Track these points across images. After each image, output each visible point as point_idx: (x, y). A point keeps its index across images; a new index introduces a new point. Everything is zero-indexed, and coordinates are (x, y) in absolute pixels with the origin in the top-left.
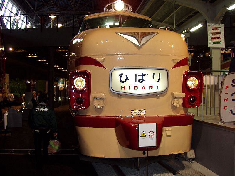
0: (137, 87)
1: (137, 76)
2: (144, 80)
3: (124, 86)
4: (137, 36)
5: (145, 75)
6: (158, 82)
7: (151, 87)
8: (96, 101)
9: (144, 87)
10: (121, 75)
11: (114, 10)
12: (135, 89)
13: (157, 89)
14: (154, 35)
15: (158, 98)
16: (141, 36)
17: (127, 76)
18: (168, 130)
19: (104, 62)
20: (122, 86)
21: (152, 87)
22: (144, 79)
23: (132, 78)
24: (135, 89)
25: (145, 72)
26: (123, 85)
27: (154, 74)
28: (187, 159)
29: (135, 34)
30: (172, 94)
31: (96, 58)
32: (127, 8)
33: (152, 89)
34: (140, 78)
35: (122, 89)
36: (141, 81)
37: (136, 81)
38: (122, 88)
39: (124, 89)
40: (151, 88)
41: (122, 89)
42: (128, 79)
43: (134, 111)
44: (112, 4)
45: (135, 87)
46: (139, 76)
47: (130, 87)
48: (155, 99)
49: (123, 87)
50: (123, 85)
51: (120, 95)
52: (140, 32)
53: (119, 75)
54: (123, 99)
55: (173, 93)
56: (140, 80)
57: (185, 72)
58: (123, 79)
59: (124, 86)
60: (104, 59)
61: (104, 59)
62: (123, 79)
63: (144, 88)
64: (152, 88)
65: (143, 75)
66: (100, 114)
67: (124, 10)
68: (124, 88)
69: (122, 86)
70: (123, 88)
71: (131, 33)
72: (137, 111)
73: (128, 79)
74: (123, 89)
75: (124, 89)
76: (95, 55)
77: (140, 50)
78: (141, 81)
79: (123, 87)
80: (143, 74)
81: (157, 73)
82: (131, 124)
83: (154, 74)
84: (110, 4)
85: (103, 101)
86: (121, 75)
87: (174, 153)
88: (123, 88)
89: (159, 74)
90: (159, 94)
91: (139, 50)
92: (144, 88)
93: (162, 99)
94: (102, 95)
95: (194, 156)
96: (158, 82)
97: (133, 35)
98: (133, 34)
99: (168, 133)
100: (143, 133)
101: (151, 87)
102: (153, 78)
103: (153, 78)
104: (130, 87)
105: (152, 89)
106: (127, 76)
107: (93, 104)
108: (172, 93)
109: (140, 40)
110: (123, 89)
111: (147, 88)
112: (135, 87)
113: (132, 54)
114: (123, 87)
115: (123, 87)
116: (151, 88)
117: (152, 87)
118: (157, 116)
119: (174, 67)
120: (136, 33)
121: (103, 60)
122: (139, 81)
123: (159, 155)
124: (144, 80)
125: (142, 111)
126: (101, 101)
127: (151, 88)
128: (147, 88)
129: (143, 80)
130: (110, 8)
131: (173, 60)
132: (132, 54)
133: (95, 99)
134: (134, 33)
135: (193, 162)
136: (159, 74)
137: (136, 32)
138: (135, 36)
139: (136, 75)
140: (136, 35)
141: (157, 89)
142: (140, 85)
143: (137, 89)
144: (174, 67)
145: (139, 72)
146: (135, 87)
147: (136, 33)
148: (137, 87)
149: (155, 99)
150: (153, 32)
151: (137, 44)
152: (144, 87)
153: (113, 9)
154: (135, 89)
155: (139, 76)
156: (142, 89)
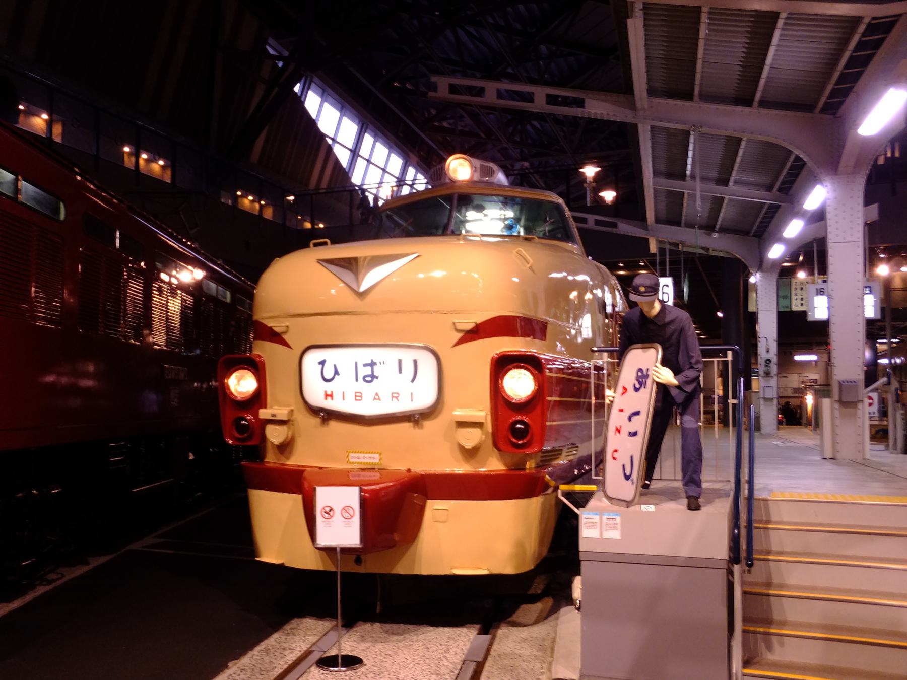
1: (360, 367)
2: (377, 378)
5: (378, 363)
9: (377, 394)
10: (322, 363)
12: (357, 398)
22: (375, 374)
23: (347, 372)
24: (356, 400)
26: (329, 387)
34: (368, 370)
37: (357, 380)
38: (327, 395)
46: (365, 365)
50: (329, 387)
51: (328, 416)
61: (287, 327)
62: (329, 374)
64: (397, 398)
65: (372, 364)
66: (288, 458)
68: (331, 396)
76: (270, 318)
78: (369, 379)
81: (407, 356)
86: (322, 363)
89: (415, 362)
91: (362, 300)
92: (377, 397)
93: (429, 425)
94: (282, 413)
111: (385, 395)
118: (409, 471)
119: (460, 342)
124: (377, 378)
127: (395, 396)
128: (385, 395)
129: (373, 377)
136: (415, 362)
142: (368, 390)
143: (360, 398)
144: (460, 342)
145: (364, 355)
146: (358, 394)
152: (377, 394)
154: (357, 398)
155: (365, 365)
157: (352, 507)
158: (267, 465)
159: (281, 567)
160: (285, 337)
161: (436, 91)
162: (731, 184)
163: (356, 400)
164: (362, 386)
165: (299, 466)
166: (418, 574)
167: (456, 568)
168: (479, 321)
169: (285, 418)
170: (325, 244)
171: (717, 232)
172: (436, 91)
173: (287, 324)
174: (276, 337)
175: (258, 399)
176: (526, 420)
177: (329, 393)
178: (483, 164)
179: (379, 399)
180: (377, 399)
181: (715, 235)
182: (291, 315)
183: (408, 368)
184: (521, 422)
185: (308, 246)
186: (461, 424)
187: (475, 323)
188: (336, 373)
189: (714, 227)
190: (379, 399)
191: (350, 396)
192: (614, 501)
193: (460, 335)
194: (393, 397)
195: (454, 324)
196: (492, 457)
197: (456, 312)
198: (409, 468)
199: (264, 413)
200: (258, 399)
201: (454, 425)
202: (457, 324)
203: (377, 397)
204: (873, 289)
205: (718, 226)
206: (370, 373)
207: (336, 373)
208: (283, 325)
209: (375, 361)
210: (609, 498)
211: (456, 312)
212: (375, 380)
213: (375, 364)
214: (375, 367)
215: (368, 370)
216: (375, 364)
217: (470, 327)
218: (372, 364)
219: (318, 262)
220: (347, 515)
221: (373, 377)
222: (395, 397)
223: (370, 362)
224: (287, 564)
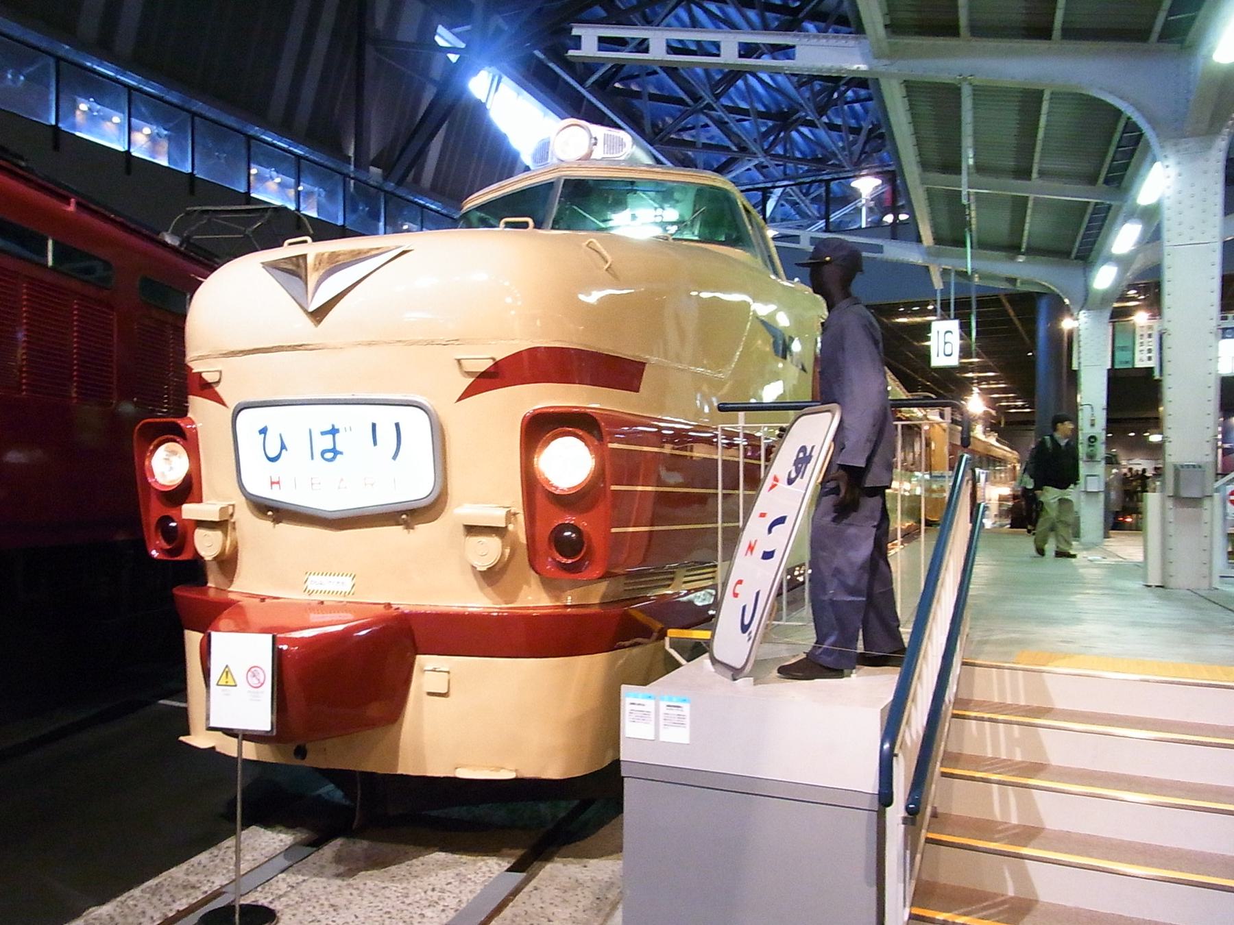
1: (316, 435)
2: (341, 453)
4: (304, 271)
10: (263, 431)
15: (408, 526)
18: (434, 670)
22: (338, 448)
23: (299, 445)
29: (298, 266)
34: (327, 442)
46: (323, 433)
48: (399, 529)
54: (285, 528)
56: (329, 451)
65: (334, 431)
78: (329, 455)
81: (385, 417)
86: (263, 431)
87: (464, 774)
91: (316, 326)
93: (422, 529)
100: (227, 671)
113: (294, 348)
119: (468, 393)
123: (399, 772)
126: (217, 535)
132: (294, 348)
134: (297, 257)
144: (468, 393)
149: (395, 532)
150: (378, 249)
155: (323, 433)
157: (261, 666)
160: (218, 389)
161: (578, 47)
162: (1035, 175)
169: (216, 519)
171: (1023, 254)
172: (578, 47)
174: (207, 389)
175: (188, 489)
176: (583, 524)
177: (275, 480)
178: (610, 133)
181: (1021, 259)
183: (387, 436)
184: (574, 528)
186: (472, 530)
188: (283, 447)
189: (1020, 248)
192: (718, 666)
193: (471, 380)
195: (459, 361)
196: (528, 584)
199: (190, 511)
200: (188, 489)
201: (462, 529)
205: (1024, 246)
207: (283, 447)
209: (336, 427)
210: (714, 661)
212: (339, 456)
213: (337, 431)
214: (337, 435)
215: (327, 442)
216: (337, 431)
218: (334, 431)
219: (263, 267)
220: (254, 682)
221: (335, 452)
224: (218, 749)
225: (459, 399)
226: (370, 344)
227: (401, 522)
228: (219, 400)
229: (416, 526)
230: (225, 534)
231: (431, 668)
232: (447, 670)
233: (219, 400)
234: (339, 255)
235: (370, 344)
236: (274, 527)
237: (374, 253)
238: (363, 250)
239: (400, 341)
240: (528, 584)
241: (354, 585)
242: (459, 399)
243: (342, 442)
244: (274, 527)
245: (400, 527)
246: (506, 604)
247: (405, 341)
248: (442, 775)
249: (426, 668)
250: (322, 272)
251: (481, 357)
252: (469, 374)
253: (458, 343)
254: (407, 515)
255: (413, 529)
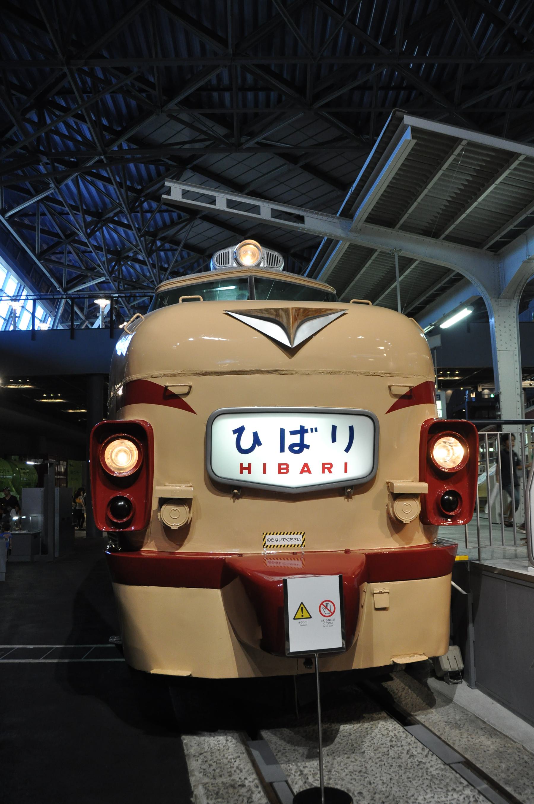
0: (285, 466)
1: (287, 434)
2: (308, 447)
3: (250, 465)
5: (309, 431)
6: (347, 450)
7: (326, 466)
8: (166, 508)
9: (306, 465)
10: (239, 431)
11: (235, 265)
12: (282, 471)
13: (346, 471)
14: (333, 317)
15: (349, 496)
16: (295, 319)
17: (255, 435)
19: (189, 396)
20: (241, 465)
21: (329, 466)
22: (306, 443)
24: (280, 472)
25: (308, 421)
26: (246, 459)
27: (334, 428)
28: (439, 675)
29: (278, 315)
30: (389, 486)
31: (167, 384)
32: (272, 261)
33: (330, 472)
34: (296, 439)
35: (241, 472)
36: (297, 448)
37: (282, 450)
38: (242, 468)
39: (250, 472)
40: (326, 471)
41: (241, 472)
42: (260, 444)
43: (271, 537)
44: (231, 250)
45: (282, 467)
46: (293, 433)
47: (265, 465)
48: (340, 500)
49: (246, 465)
50: (246, 459)
52: (292, 308)
53: (235, 432)
54: (245, 503)
55: (392, 484)
57: (426, 422)
58: (246, 443)
59: (250, 465)
60: (190, 387)
61: (190, 387)
62: (246, 443)
63: (306, 469)
65: (302, 431)
66: (180, 545)
67: (262, 265)
68: (249, 469)
69: (241, 465)
70: (246, 469)
71: (266, 310)
72: (278, 537)
73: (260, 444)
74: (245, 472)
75: (250, 472)
76: (165, 376)
77: (293, 359)
78: (297, 448)
79: (246, 465)
80: (302, 427)
82: (266, 577)
83: (334, 428)
84: (226, 250)
85: (187, 508)
86: (239, 431)
88: (246, 469)
89: (351, 429)
90: (351, 487)
91: (290, 359)
92: (306, 469)
95: (462, 666)
96: (347, 450)
97: (271, 317)
98: (272, 314)
99: (381, 601)
101: (326, 466)
102: (334, 440)
103: (334, 440)
104: (265, 465)
105: (330, 472)
106: (255, 435)
107: (159, 517)
108: (388, 483)
109: (292, 331)
110: (245, 472)
111: (316, 468)
112: (280, 465)
114: (244, 466)
115: (244, 466)
116: (326, 471)
117: (331, 465)
118: (347, 551)
119: (393, 408)
120: (281, 312)
121: (186, 390)
122: (291, 448)
124: (308, 447)
125: (295, 536)
127: (327, 467)
128: (316, 468)
129: (302, 446)
130: (224, 260)
131: (389, 387)
133: (163, 501)
134: (277, 310)
135: (457, 683)
137: (282, 309)
138: (278, 319)
139: (282, 431)
140: (282, 317)
141: (346, 471)
143: (285, 471)
144: (393, 408)
146: (282, 467)
147: (280, 310)
148: (285, 466)
150: (331, 310)
151: (285, 340)
152: (306, 465)
153: (232, 264)
154: (282, 471)
155: (293, 433)
156: (302, 471)
158: (142, 554)
159: (189, 679)
160: (187, 400)
163: (280, 472)
164: (288, 457)
165: (198, 554)
166: (357, 668)
167: (395, 656)
168: (415, 384)
170: (198, 300)
173: (190, 383)
179: (309, 471)
180: (306, 471)
182: (196, 374)
185: (177, 302)
186: (397, 497)
187: (410, 387)
188: (257, 441)
190: (309, 471)
191: (273, 469)
193: (396, 400)
194: (324, 469)
197: (389, 375)
198: (347, 548)
202: (392, 388)
203: (306, 469)
204: (441, 398)
206: (298, 441)
207: (257, 441)
208: (187, 384)
211: (389, 375)
212: (305, 449)
213: (306, 431)
214: (306, 435)
216: (306, 431)
217: (404, 391)
222: (327, 468)
223: (299, 429)
224: (194, 676)
225: (389, 411)
226: (331, 373)
227: (346, 494)
228: (187, 408)
229: (353, 497)
230: (190, 509)
231: (379, 592)
232: (388, 591)
233: (187, 408)
234: (309, 311)
235: (331, 373)
236: (234, 502)
237: (329, 312)
238: (323, 309)
239: (352, 372)
240: (419, 533)
241: (304, 540)
242: (389, 411)
243: (308, 438)
244: (234, 502)
245: (342, 498)
246: (407, 545)
247: (356, 372)
248: (382, 665)
249: (375, 592)
250: (299, 321)
251: (403, 385)
252: (395, 396)
253: (390, 375)
254: (352, 489)
255: (351, 498)
